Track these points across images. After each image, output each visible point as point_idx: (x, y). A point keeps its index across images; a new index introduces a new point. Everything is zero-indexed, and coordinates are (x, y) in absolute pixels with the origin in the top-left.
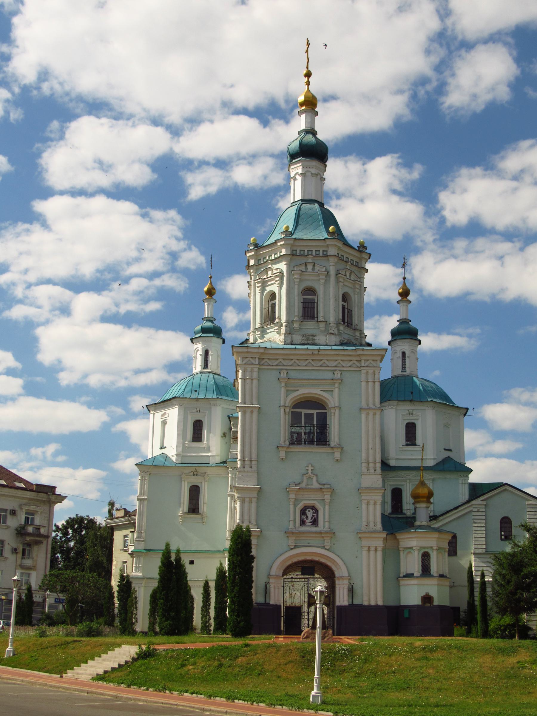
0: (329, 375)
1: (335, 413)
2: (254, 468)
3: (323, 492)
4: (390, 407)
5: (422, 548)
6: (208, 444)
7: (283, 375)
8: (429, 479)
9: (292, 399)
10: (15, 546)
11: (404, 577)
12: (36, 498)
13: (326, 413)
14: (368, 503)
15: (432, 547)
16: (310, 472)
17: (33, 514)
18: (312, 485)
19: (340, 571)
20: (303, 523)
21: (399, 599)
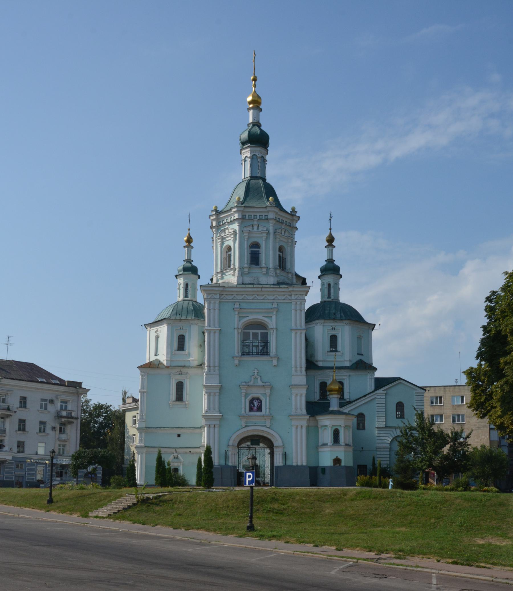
0: (269, 306)
1: (273, 332)
2: (217, 372)
3: (265, 388)
4: (319, 324)
5: (333, 426)
7: (237, 306)
8: (346, 375)
9: (244, 322)
10: (54, 425)
11: (321, 445)
12: (68, 391)
13: (267, 333)
14: (296, 395)
15: (341, 425)
16: (256, 374)
17: (66, 402)
18: (257, 383)
19: (277, 442)
20: (251, 409)
21: (318, 461)
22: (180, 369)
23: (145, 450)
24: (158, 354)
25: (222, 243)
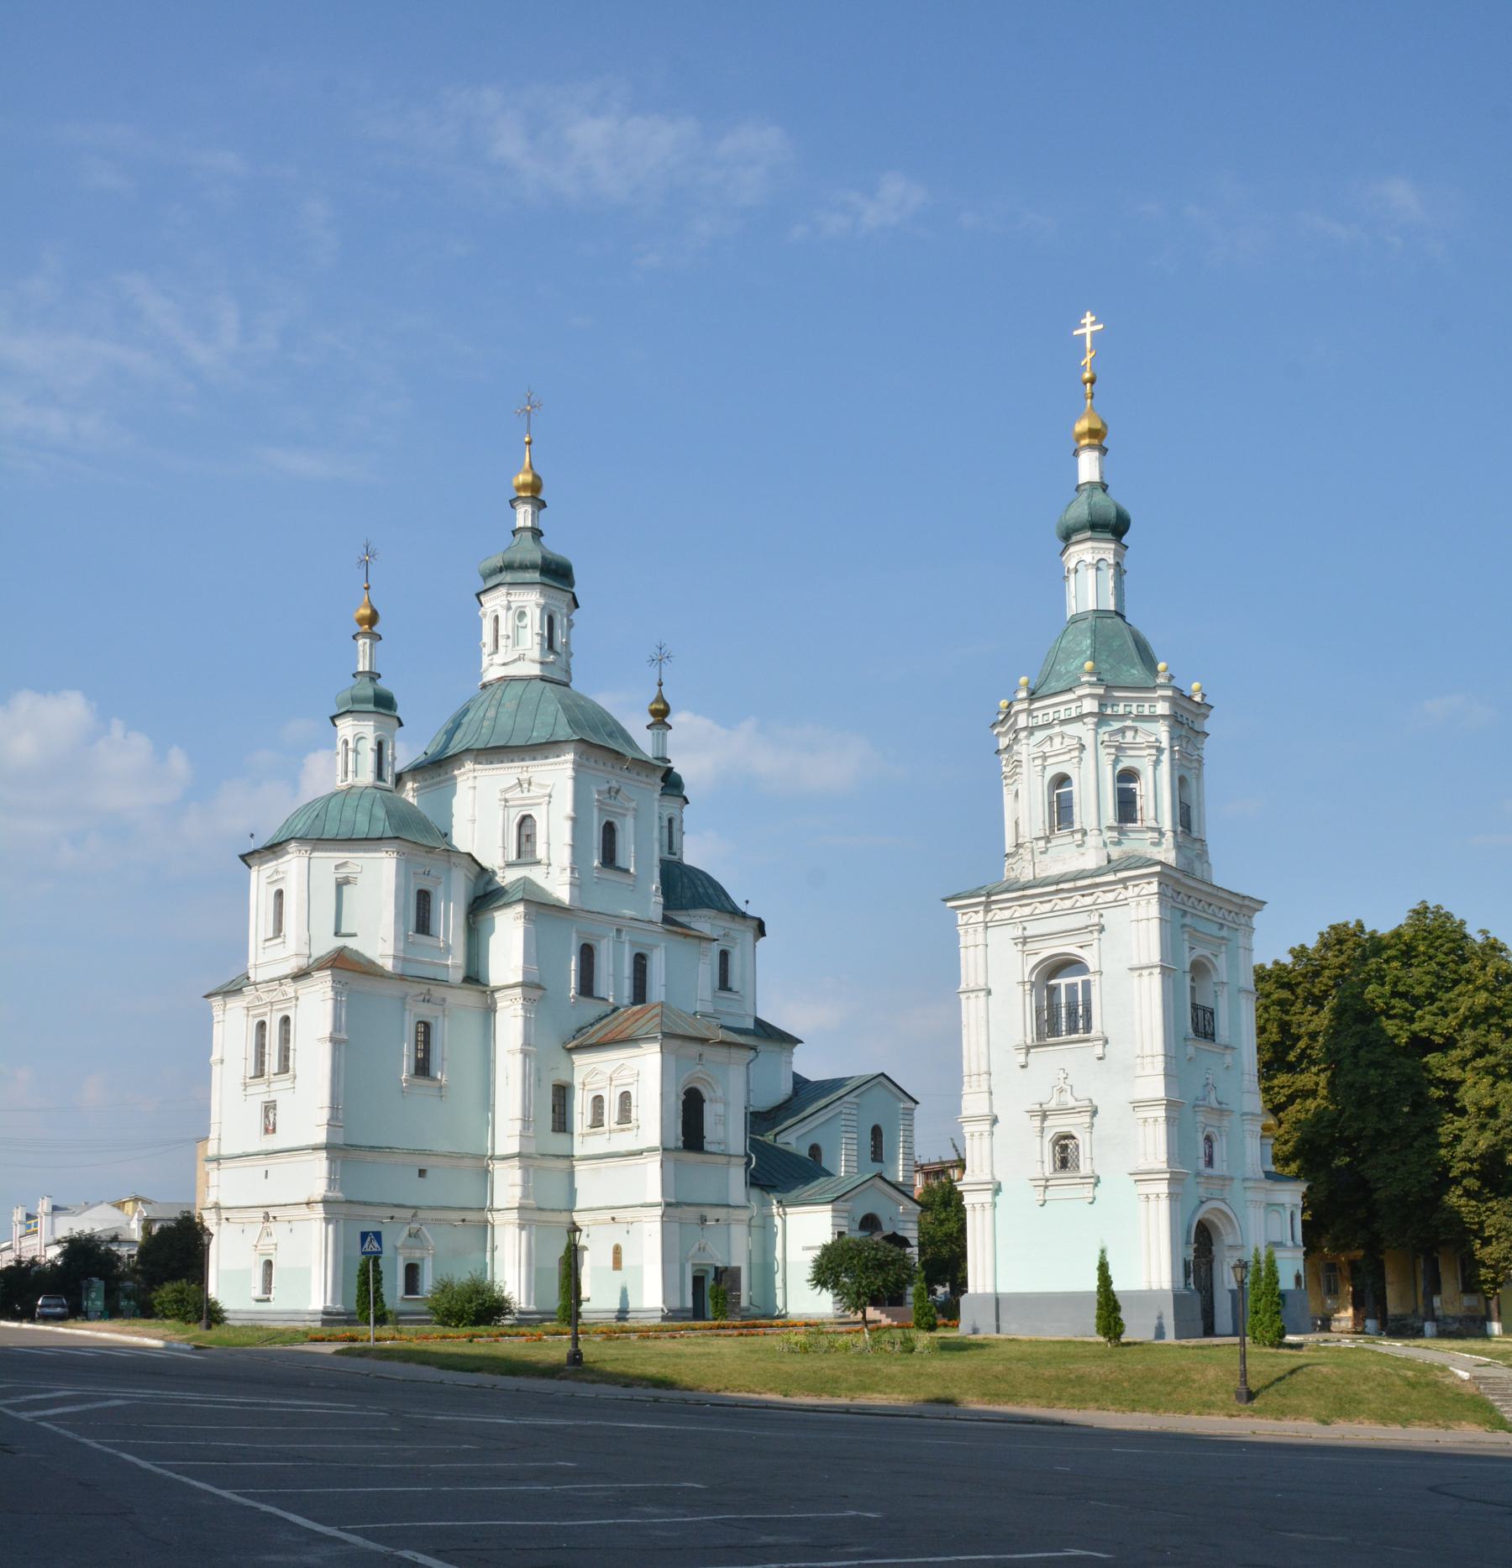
0: (1214, 930)
6: (446, 942)
22: (427, 987)
23: (344, 1209)
24: (344, 930)
25: (1116, 761)
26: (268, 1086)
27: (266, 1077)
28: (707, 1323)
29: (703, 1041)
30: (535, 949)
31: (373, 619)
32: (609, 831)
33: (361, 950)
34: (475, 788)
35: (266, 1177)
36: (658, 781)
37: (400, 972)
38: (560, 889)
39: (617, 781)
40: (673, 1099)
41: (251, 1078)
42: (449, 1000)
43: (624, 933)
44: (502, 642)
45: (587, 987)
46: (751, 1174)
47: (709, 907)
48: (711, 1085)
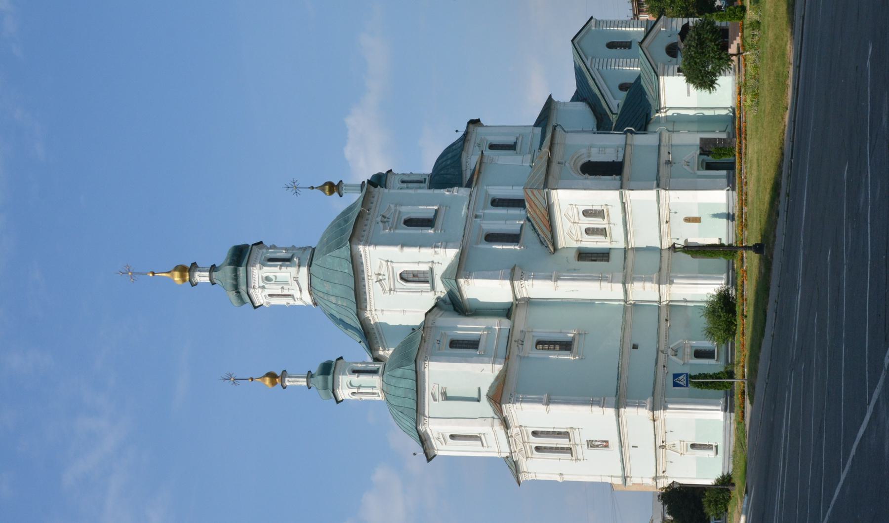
4: (469, 160)
6: (484, 330)
22: (513, 342)
23: (658, 397)
24: (476, 396)
26: (578, 445)
27: (572, 446)
28: (737, 161)
29: (549, 161)
30: (488, 271)
31: (272, 376)
32: (410, 222)
33: (489, 385)
34: (382, 310)
35: (636, 447)
36: (376, 189)
37: (504, 360)
38: (447, 256)
39: (377, 217)
40: (588, 182)
41: (572, 456)
42: (522, 328)
43: (478, 213)
44: (286, 292)
45: (513, 238)
46: (639, 130)
47: (460, 157)
48: (579, 157)
